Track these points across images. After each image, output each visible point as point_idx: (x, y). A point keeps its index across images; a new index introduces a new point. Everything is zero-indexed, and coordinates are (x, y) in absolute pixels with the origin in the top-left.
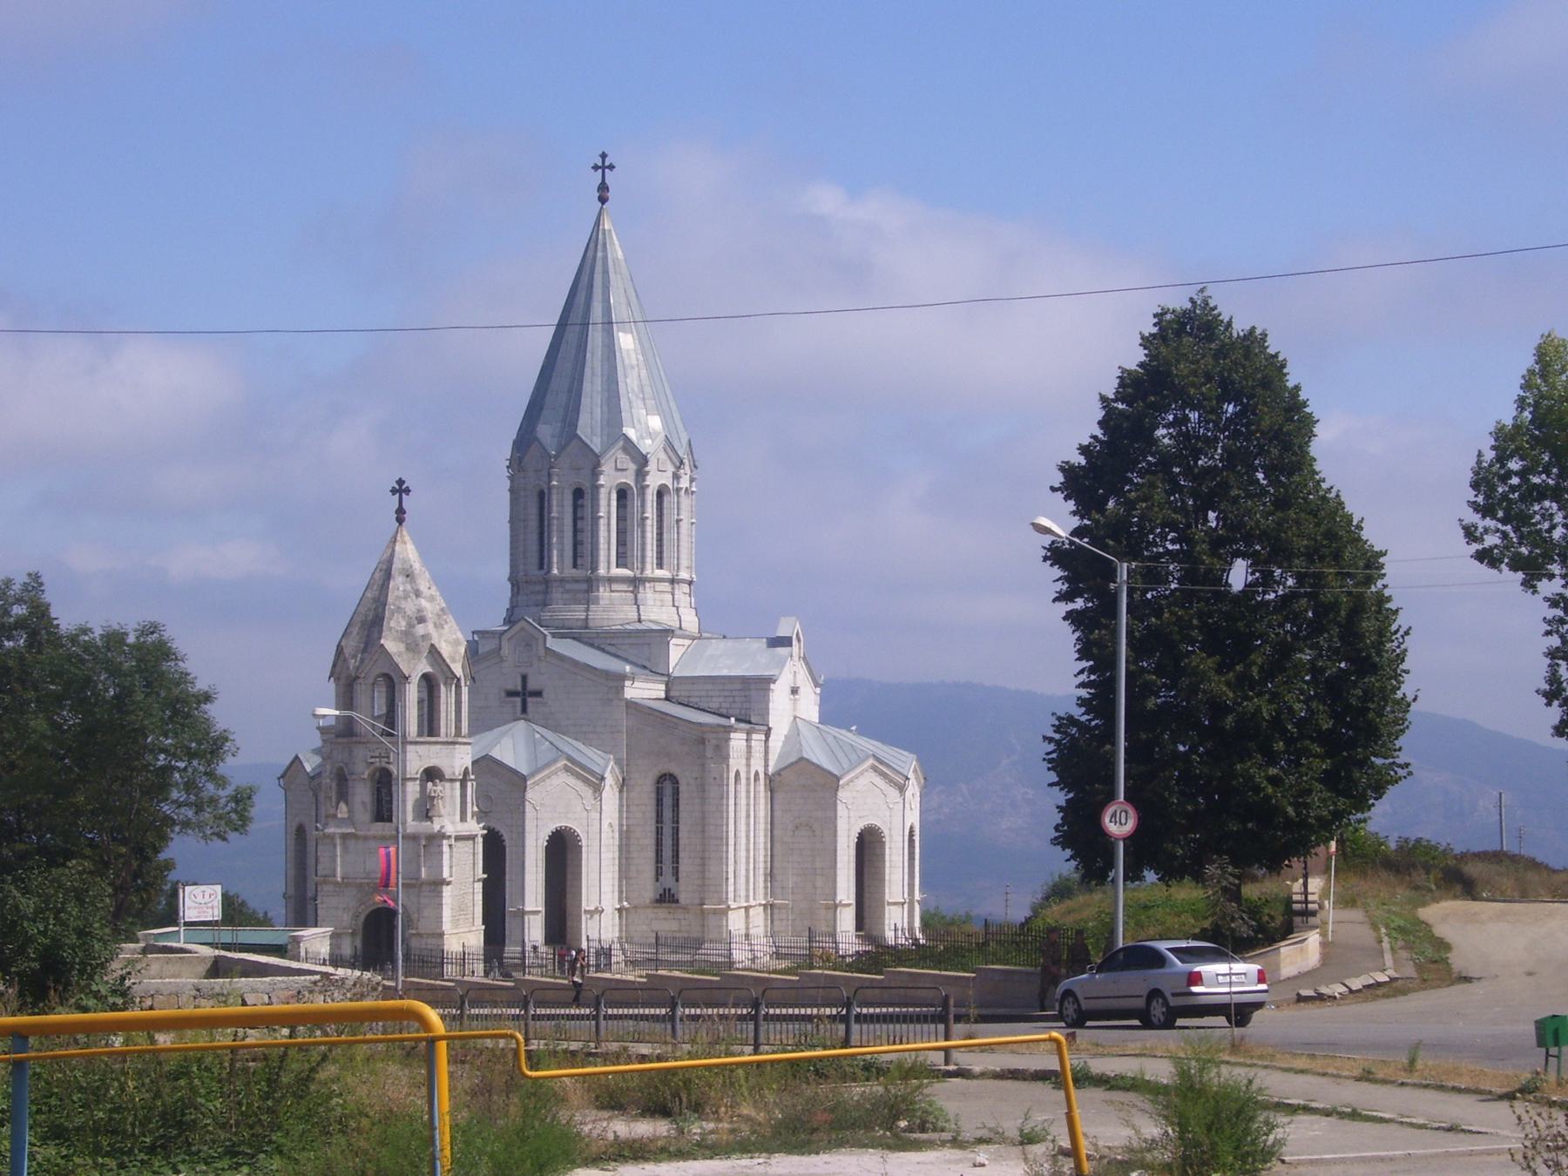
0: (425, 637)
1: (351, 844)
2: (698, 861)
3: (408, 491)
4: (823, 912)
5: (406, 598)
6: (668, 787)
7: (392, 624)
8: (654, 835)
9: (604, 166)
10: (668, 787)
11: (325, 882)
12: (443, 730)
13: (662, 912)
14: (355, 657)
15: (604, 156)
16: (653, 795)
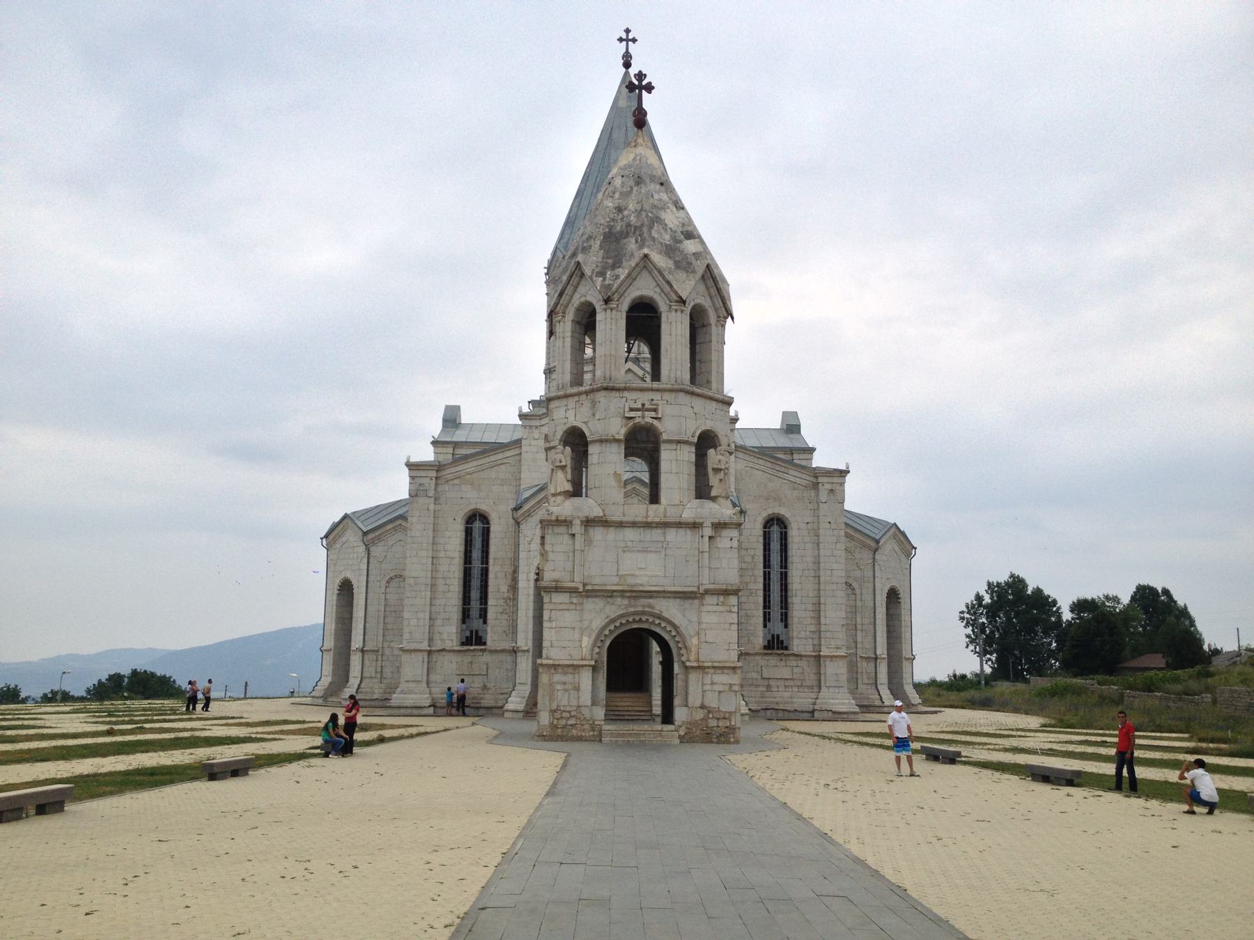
0: (697, 255)
1: (597, 533)
2: (810, 607)
3: (649, 88)
4: (865, 664)
5: (664, 208)
6: (775, 530)
7: (655, 234)
8: (761, 580)
9: (627, 38)
10: (775, 530)
11: (558, 589)
12: (714, 385)
13: (773, 660)
14: (602, 274)
15: (628, 31)
16: (761, 540)
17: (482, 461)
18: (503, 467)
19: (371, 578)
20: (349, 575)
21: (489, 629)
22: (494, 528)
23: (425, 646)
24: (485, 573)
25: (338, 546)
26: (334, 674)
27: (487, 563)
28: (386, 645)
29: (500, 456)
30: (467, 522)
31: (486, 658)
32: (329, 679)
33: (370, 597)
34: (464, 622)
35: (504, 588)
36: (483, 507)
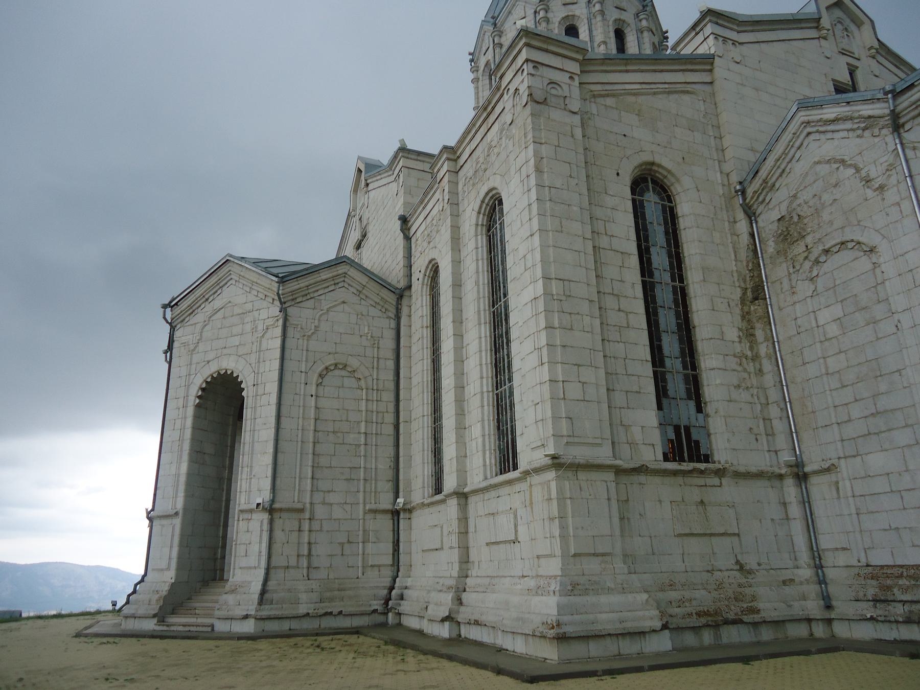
17: (649, 77)
18: (686, 98)
19: (287, 363)
20: (229, 364)
21: (716, 424)
22: (687, 208)
23: (603, 455)
24: (682, 298)
25: (200, 317)
26: (179, 568)
27: (681, 280)
28: (318, 497)
29: (680, 77)
30: (633, 192)
31: (729, 491)
32: (170, 576)
33: (287, 399)
34: (660, 407)
35: (732, 334)
36: (665, 162)
